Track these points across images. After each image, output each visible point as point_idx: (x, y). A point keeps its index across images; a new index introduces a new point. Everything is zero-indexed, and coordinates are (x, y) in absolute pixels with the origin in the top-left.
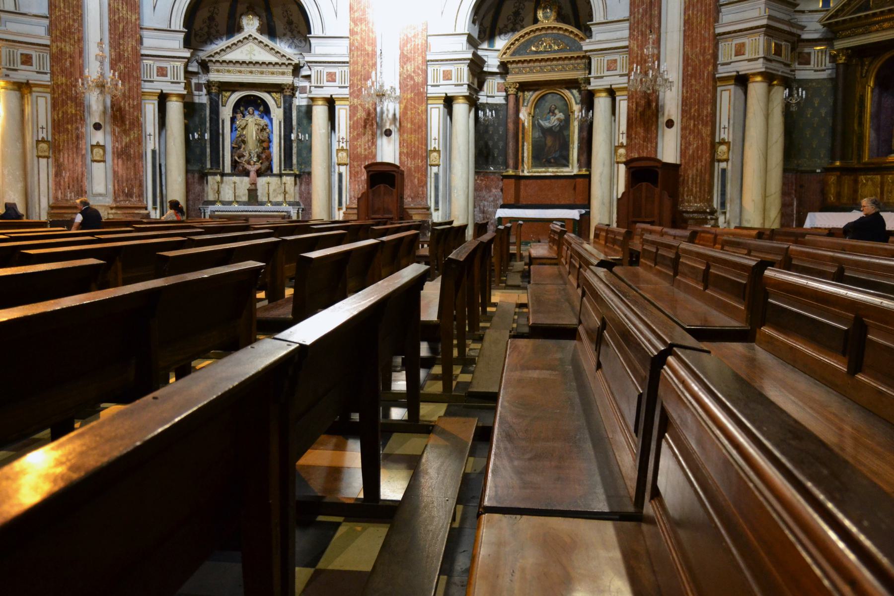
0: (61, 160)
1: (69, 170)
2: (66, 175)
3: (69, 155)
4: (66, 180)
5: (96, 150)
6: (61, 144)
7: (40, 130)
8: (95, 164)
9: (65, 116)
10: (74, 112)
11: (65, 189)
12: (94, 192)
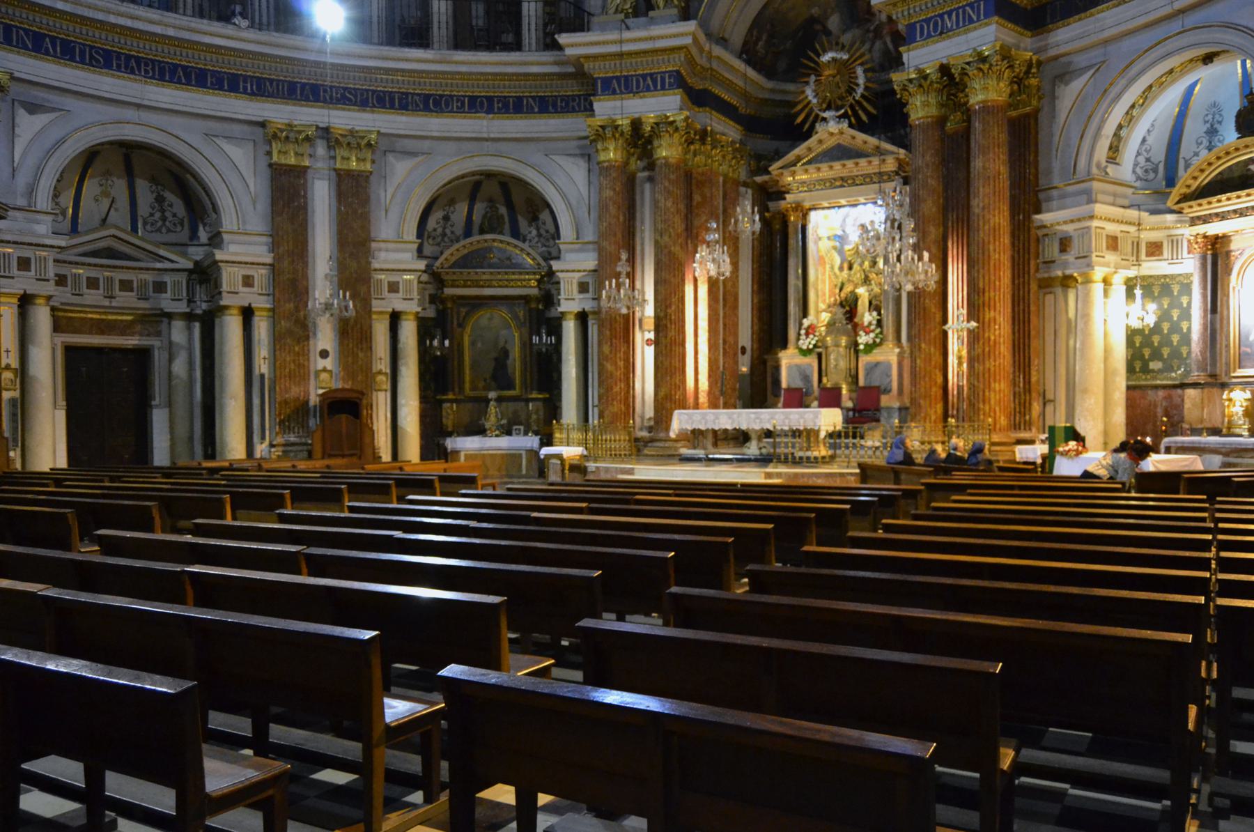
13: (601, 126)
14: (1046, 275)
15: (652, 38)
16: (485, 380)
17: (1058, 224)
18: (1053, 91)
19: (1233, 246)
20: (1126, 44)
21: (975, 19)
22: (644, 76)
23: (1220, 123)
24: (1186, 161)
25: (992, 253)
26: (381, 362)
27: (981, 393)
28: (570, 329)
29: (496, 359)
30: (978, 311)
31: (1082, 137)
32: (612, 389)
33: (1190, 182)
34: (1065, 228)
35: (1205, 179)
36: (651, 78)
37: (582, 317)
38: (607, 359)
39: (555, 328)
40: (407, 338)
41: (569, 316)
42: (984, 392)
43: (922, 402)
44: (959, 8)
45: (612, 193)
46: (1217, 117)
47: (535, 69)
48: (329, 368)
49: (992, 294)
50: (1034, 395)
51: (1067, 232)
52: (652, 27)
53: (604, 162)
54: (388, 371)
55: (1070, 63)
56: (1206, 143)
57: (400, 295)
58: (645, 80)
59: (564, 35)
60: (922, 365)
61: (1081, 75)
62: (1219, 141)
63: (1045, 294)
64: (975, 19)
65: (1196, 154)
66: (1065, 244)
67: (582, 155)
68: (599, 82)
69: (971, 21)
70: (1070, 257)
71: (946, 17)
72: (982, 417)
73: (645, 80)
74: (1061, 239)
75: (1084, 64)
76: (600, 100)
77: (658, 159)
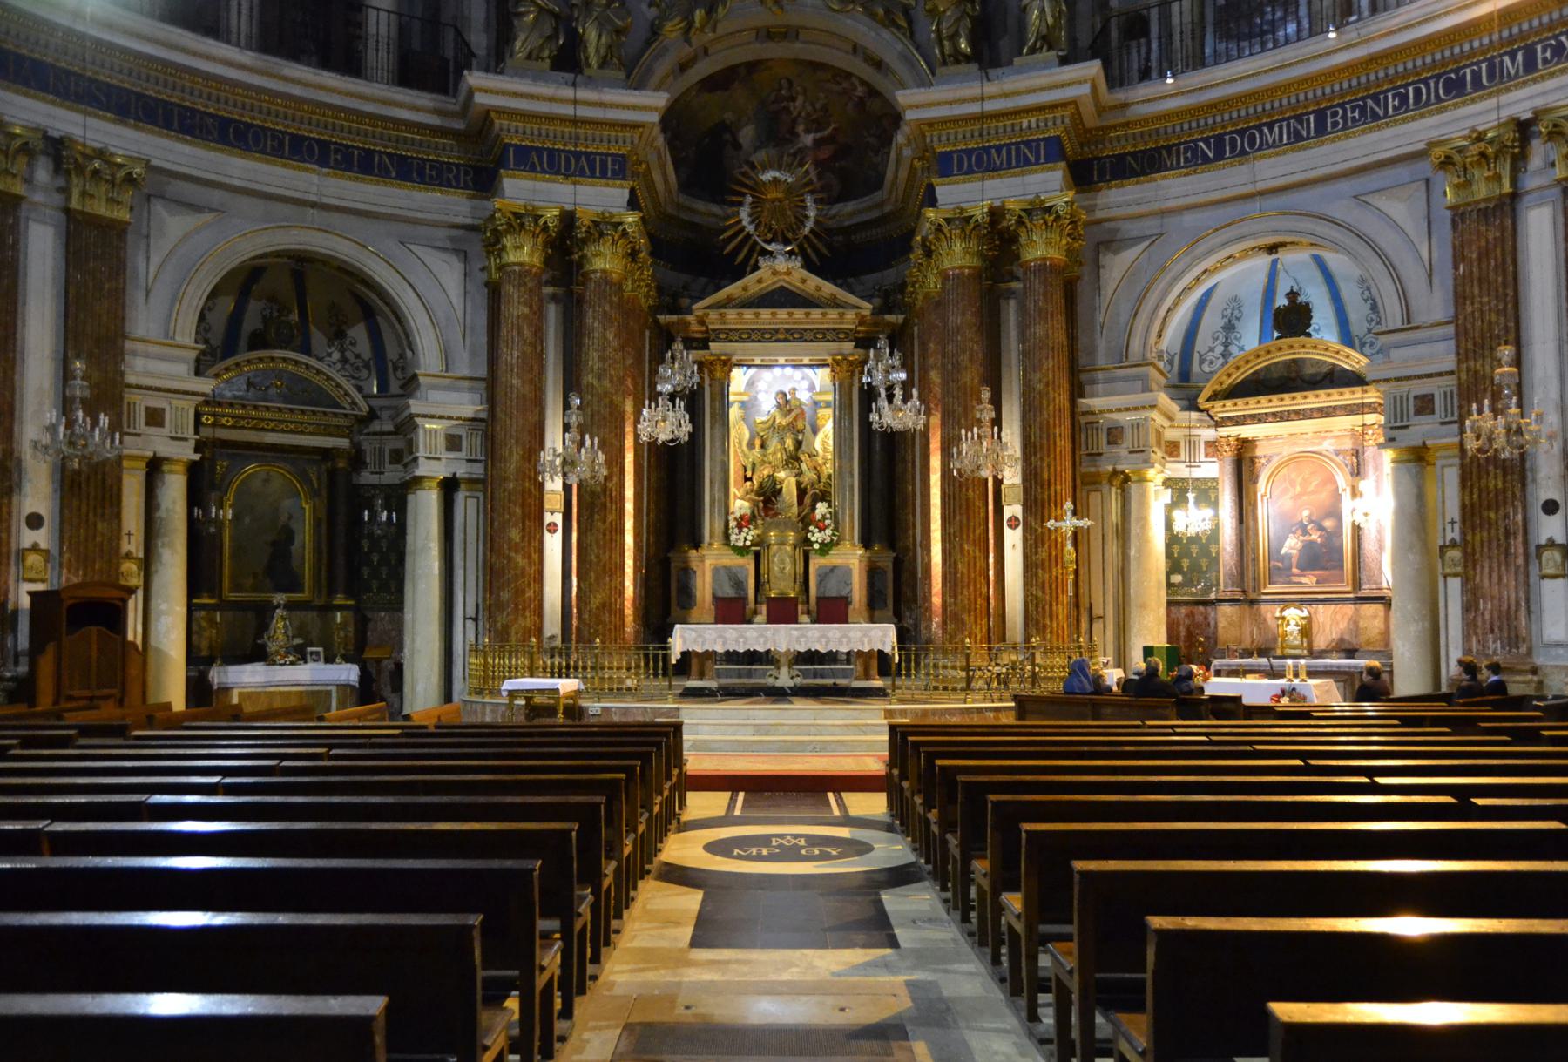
0: (1478, 578)
1: (1492, 598)
2: (1486, 607)
3: (1491, 567)
4: (1487, 616)
5: (1546, 555)
6: (1478, 549)
7: (1449, 527)
8: (1547, 583)
9: (1484, 496)
10: (1500, 485)
11: (1484, 634)
12: (1546, 638)
13: (514, 214)
14: (1093, 470)
15: (602, 105)
16: (255, 575)
17: (1111, 411)
18: (1097, 260)
19: (1258, 452)
20: (1189, 219)
21: (1032, 159)
22: (578, 155)
23: (1238, 319)
24: (1201, 356)
25: (1058, 439)
26: (133, 544)
27: (1047, 607)
28: (426, 507)
29: (274, 544)
30: (1043, 507)
31: (1136, 315)
32: (523, 592)
33: (1224, 378)
34: (1115, 416)
35: (1238, 377)
36: (587, 160)
37: (449, 487)
38: (516, 548)
39: (399, 496)
40: (174, 502)
41: (426, 484)
42: (1051, 605)
43: (965, 617)
44: (1012, 144)
45: (526, 310)
46: (1236, 312)
47: (404, 114)
48: (43, 545)
49: (1059, 488)
50: (1082, 610)
51: (1117, 421)
52: (606, 89)
53: (515, 264)
54: (141, 555)
55: (1118, 230)
56: (1222, 339)
57: (166, 431)
58: (578, 161)
59: (476, 74)
60: (965, 571)
61: (1133, 245)
62: (1236, 338)
63: (1089, 492)
64: (1032, 159)
65: (1212, 350)
66: (1115, 435)
67: (456, 251)
68: (511, 150)
69: (1027, 163)
70: (1122, 451)
72: (1049, 636)
73: (578, 161)
74: (1109, 429)
75: (1135, 233)
77: (595, 271)
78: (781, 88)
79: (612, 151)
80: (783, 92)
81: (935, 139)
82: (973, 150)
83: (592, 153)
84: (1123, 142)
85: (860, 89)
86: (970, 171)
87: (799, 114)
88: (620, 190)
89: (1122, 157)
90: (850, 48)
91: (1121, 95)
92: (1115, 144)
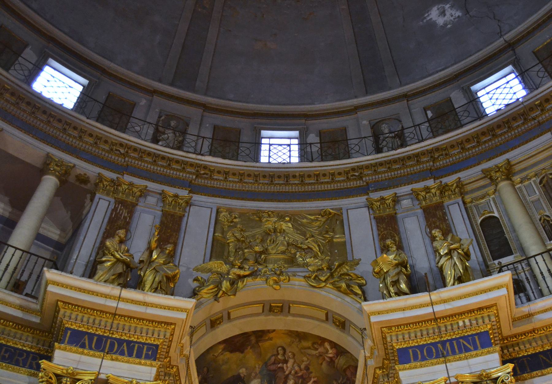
44: (452, 340)
71: (439, 345)
76: (65, 349)
78: (278, 354)
79: (149, 341)
80: (280, 357)
81: (394, 338)
82: (424, 346)
83: (132, 342)
84: (534, 344)
85: (330, 351)
86: (424, 359)
87: (291, 372)
88: (149, 368)
89: (535, 356)
90: (324, 318)
91: (526, 308)
92: (528, 346)
